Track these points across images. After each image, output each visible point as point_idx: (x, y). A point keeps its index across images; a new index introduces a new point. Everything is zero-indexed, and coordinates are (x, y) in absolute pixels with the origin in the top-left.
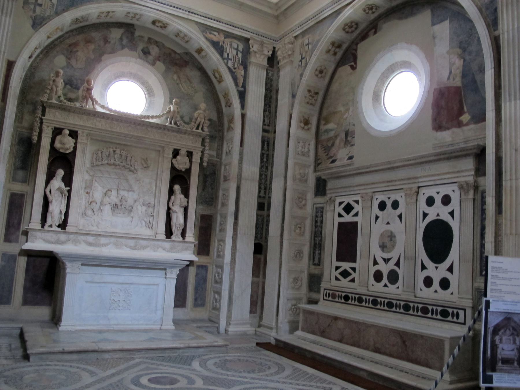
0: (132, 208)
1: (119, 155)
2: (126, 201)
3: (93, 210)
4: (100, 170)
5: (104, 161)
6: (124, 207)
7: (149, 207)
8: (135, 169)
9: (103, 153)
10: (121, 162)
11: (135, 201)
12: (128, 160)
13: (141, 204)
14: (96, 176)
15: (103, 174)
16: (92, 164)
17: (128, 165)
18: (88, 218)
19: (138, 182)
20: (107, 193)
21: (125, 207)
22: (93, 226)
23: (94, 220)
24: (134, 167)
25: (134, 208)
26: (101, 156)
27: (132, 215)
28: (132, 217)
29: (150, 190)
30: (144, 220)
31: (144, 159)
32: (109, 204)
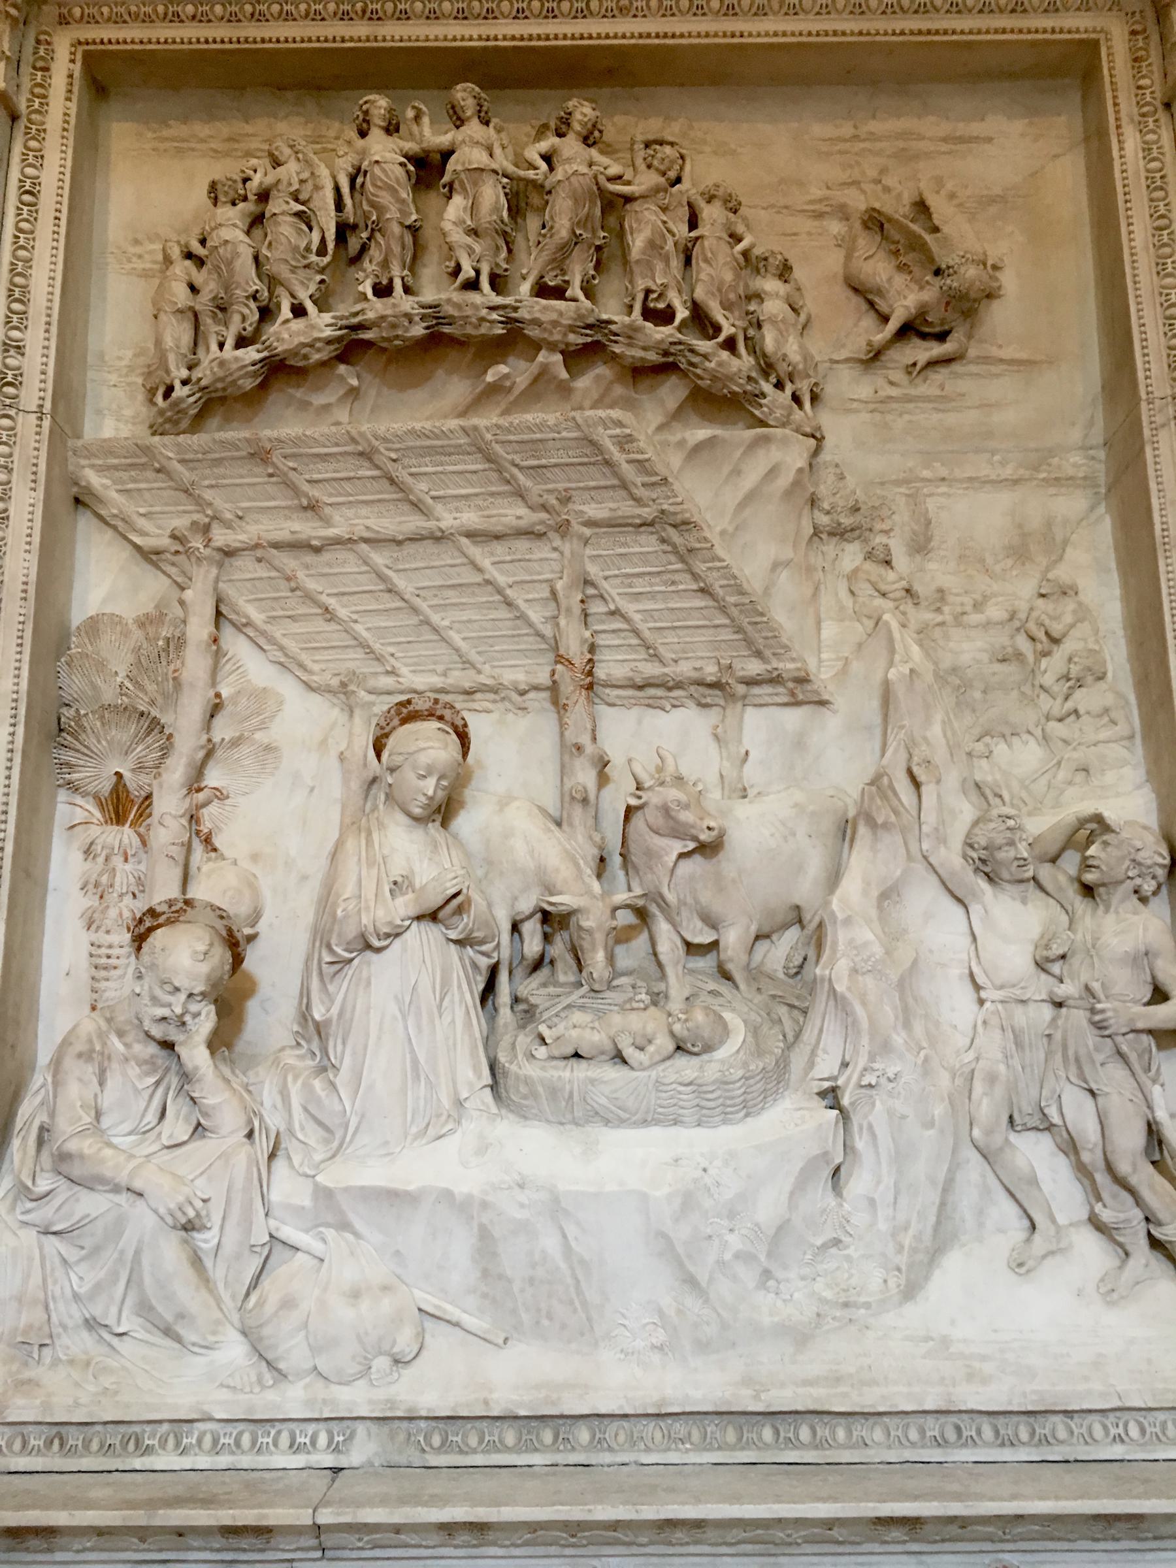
0: (818, 940)
1: (492, 196)
2: (708, 849)
3: (168, 1046)
4: (260, 455)
5: (299, 311)
6: (691, 948)
7: (1088, 890)
8: (767, 367)
9: (278, 205)
10: (542, 290)
11: (845, 831)
12: (637, 243)
13: (951, 857)
14: (228, 553)
15: (312, 507)
16: (152, 392)
17: (664, 317)
18: (92, 1204)
19: (851, 556)
20: (385, 756)
21: (706, 938)
22: (168, 1332)
23: (189, 1227)
24: (753, 347)
25: (839, 937)
26: (245, 266)
27: (826, 1066)
28: (831, 1096)
29: (1055, 641)
30: (1050, 1128)
31: (875, 222)
32: (433, 916)
